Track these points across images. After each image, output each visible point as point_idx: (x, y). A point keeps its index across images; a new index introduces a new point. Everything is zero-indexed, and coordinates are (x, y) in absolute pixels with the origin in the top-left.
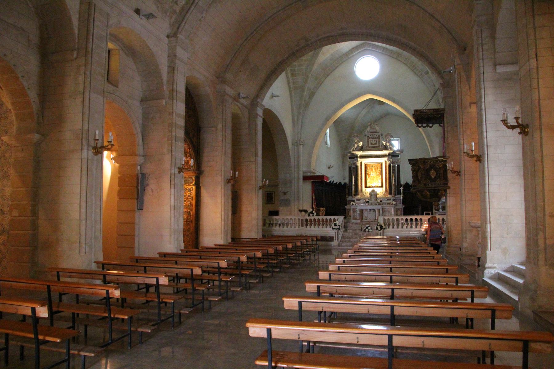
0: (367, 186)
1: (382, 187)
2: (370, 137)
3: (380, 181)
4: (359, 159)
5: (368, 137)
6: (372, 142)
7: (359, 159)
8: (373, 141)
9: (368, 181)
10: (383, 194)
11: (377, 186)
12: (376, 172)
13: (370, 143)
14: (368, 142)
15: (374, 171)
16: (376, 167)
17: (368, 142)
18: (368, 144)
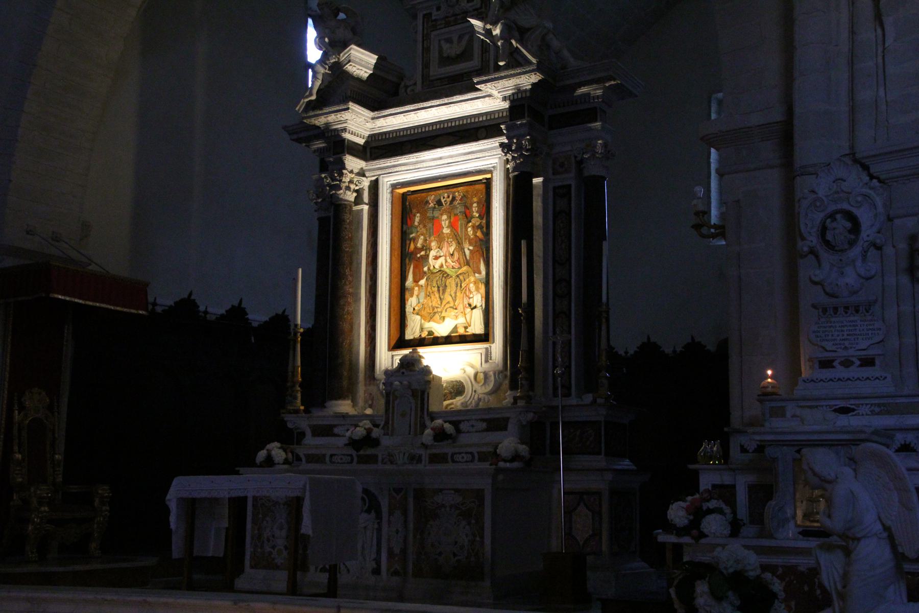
0: (409, 336)
1: (485, 337)
2: (435, 15)
3: (478, 299)
4: (353, 163)
5: (427, 16)
6: (445, 46)
7: (353, 163)
8: (449, 41)
9: (412, 302)
10: (491, 385)
11: (461, 331)
12: (460, 244)
13: (434, 55)
14: (426, 50)
15: (446, 231)
16: (460, 209)
17: (426, 50)
18: (426, 66)
